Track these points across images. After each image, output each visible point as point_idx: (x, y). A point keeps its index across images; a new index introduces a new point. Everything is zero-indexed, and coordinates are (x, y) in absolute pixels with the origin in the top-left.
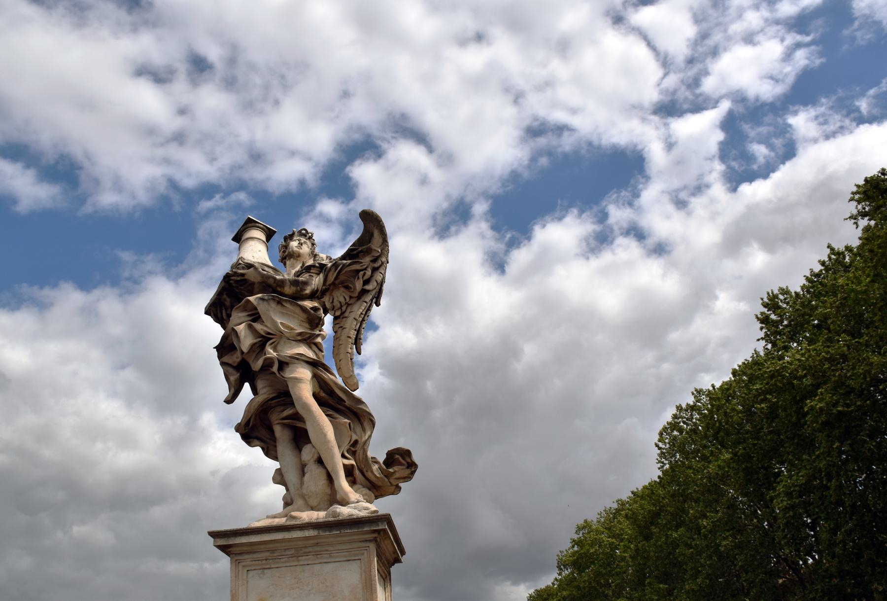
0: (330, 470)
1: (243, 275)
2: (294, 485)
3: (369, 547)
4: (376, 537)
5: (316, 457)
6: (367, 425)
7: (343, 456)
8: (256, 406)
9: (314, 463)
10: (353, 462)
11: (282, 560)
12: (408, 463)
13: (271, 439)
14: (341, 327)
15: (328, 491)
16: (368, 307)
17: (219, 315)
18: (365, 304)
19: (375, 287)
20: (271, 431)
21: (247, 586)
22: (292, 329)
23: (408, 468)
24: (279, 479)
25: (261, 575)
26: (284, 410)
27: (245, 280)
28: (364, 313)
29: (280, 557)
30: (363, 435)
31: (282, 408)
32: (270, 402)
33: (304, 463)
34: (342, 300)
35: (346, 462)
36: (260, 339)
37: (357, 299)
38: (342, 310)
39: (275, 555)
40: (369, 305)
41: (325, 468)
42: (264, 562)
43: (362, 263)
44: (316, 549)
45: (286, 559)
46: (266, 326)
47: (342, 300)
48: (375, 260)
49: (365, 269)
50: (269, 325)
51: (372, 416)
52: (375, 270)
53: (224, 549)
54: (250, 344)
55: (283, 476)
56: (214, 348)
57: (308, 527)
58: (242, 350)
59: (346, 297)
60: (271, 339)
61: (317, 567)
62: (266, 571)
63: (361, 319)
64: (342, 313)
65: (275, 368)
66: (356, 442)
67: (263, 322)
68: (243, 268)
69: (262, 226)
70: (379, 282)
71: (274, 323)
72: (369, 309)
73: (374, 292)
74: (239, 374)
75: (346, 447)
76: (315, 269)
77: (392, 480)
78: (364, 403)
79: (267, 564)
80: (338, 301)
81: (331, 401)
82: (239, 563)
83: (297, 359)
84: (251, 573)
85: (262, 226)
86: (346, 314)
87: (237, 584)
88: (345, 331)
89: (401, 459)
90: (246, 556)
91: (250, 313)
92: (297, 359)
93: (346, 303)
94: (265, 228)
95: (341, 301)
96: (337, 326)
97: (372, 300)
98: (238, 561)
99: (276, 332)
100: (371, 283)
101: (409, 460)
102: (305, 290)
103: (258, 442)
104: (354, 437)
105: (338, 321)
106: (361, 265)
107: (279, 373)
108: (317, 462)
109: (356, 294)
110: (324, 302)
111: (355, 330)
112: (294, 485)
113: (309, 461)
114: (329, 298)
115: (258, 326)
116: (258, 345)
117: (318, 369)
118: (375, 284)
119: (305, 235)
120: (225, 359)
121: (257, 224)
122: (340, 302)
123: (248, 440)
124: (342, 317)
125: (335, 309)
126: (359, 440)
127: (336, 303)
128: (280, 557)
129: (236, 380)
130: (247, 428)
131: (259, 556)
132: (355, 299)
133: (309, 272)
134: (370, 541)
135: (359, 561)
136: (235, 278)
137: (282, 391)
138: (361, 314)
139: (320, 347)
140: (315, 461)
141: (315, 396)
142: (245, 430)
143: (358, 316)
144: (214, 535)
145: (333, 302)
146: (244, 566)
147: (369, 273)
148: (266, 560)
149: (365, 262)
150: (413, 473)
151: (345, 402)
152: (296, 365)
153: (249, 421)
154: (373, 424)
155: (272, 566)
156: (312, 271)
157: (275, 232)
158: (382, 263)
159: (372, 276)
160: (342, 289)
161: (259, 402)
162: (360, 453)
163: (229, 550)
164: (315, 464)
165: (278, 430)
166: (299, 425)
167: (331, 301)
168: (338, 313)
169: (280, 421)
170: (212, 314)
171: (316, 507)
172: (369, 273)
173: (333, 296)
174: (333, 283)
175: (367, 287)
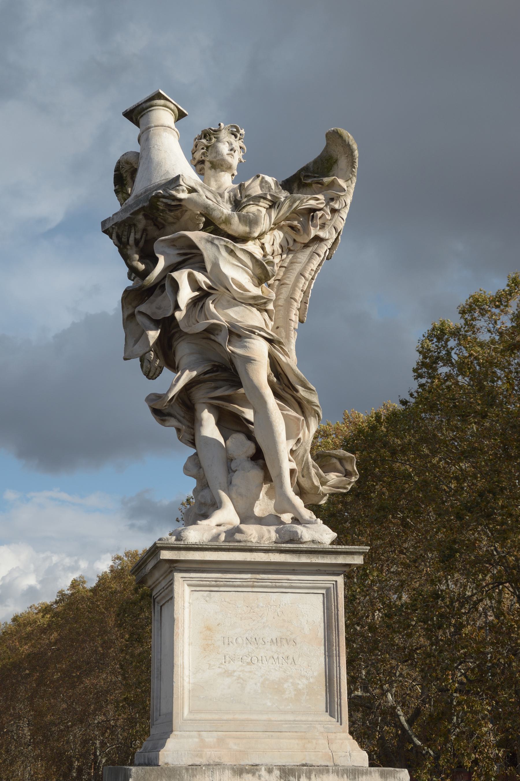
2: (220, 483)
17: (124, 239)
22: (247, 290)
25: (208, 599)
26: (216, 388)
27: (180, 205)
31: (213, 385)
33: (231, 456)
36: (197, 293)
37: (303, 245)
63: (311, 277)
69: (172, 106)
76: (265, 201)
85: (172, 106)
91: (181, 252)
94: (175, 108)
102: (254, 232)
108: (249, 459)
110: (263, 244)
133: (257, 205)
136: (169, 202)
137: (217, 364)
141: (270, 382)
156: (261, 204)
157: (186, 115)
163: (175, 565)
164: (248, 460)
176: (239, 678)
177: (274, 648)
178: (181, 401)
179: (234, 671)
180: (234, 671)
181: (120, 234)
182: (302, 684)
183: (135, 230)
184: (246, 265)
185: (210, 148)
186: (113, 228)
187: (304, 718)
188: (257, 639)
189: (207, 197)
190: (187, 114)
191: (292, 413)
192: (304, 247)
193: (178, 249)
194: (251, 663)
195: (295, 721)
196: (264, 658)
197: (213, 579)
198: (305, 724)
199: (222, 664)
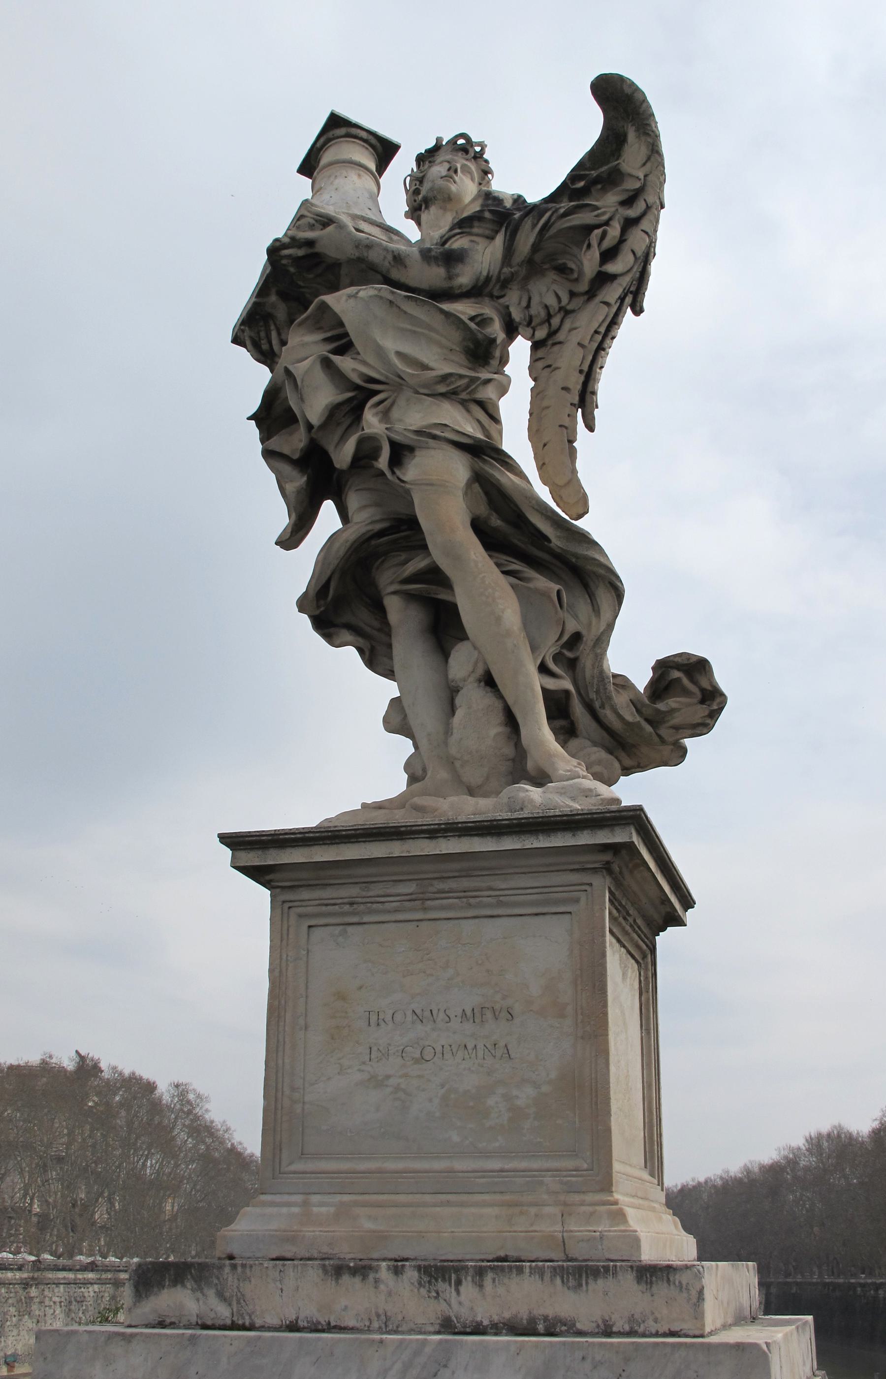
0: (510, 702)
1: (310, 243)
2: (429, 735)
3: (591, 885)
4: (608, 863)
5: (480, 671)
6: (604, 597)
7: (543, 669)
8: (342, 553)
9: (476, 685)
10: (567, 684)
11: (387, 906)
12: (703, 690)
13: (379, 630)
15: (509, 751)
16: (612, 315)
17: (265, 347)
18: (606, 308)
19: (629, 267)
20: (379, 609)
21: (307, 962)
22: (425, 367)
23: (702, 702)
24: (396, 720)
25: (341, 939)
27: (317, 255)
28: (602, 330)
29: (382, 899)
30: (594, 621)
31: (403, 556)
32: (373, 542)
34: (551, 301)
35: (552, 684)
36: (350, 394)
37: (586, 297)
38: (550, 325)
39: (371, 893)
40: (614, 309)
41: (501, 697)
42: (347, 908)
43: (596, 208)
44: (465, 883)
45: (398, 904)
46: (365, 363)
47: (551, 301)
48: (629, 201)
49: (607, 223)
50: (371, 360)
51: (618, 577)
52: (630, 223)
53: (255, 873)
54: (327, 406)
55: (406, 716)
56: (249, 419)
57: (446, 830)
58: (305, 416)
59: (560, 293)
60: (377, 392)
61: (468, 926)
62: (350, 929)
64: (552, 334)
65: (383, 462)
66: (577, 637)
67: (358, 353)
68: (312, 227)
70: (639, 253)
71: (380, 352)
72: (614, 322)
73: (625, 281)
74: (305, 478)
75: (549, 648)
77: (664, 732)
78: (596, 544)
79: (354, 914)
80: (541, 302)
81: (517, 540)
82: (290, 908)
83: (434, 437)
84: (317, 933)
86: (560, 336)
87: (284, 957)
88: (559, 375)
89: (686, 681)
90: (305, 894)
91: (329, 334)
92: (434, 437)
93: (561, 309)
94: (370, 137)
95: (548, 304)
96: (540, 364)
97: (622, 299)
98: (287, 905)
99: (387, 377)
100: (620, 258)
101: (705, 684)
102: (458, 275)
103: (347, 635)
104: (572, 626)
105: (540, 353)
106: (596, 213)
107: (393, 473)
108: (482, 684)
109: (583, 287)
110: (507, 307)
111: (581, 372)
112: (429, 735)
113: (464, 680)
115: (345, 363)
116: (346, 408)
117: (485, 461)
118: (631, 258)
119: (464, 149)
120: (276, 443)
121: (354, 131)
122: (546, 307)
123: (326, 631)
124: (550, 342)
125: (533, 324)
126: (584, 632)
127: (536, 310)
128: (382, 899)
129: (298, 492)
130: (322, 602)
131: (335, 895)
132: (582, 299)
134: (595, 870)
135: (567, 917)
138: (596, 332)
139: (491, 412)
140: (480, 681)
141: (478, 527)
142: (318, 607)
143: (589, 337)
144: (232, 841)
145: (528, 306)
146: (300, 916)
148: (351, 904)
149: (605, 207)
150: (714, 715)
151: (549, 541)
152: (432, 452)
153: (326, 587)
154: (618, 594)
155: (365, 919)
156: (475, 230)
158: (648, 207)
159: (622, 241)
160: (552, 275)
161: (347, 541)
162: (587, 662)
165: (394, 606)
166: (443, 596)
167: (524, 303)
168: (541, 334)
170: (248, 342)
171: (479, 787)
172: (614, 231)
173: (528, 291)
174: (530, 261)
175: (611, 268)
176: (397, 1089)
177: (469, 1027)
179: (388, 1077)
180: (388, 1077)
181: (257, 339)
182: (525, 1096)
183: (275, 324)
184: (430, 328)
186: (243, 331)
187: (524, 1165)
188: (435, 1013)
189: (358, 230)
191: (542, 582)
193: (325, 332)
194: (422, 1059)
195: (502, 1171)
196: (447, 1049)
197: (346, 901)
198: (523, 1177)
199: (364, 1063)
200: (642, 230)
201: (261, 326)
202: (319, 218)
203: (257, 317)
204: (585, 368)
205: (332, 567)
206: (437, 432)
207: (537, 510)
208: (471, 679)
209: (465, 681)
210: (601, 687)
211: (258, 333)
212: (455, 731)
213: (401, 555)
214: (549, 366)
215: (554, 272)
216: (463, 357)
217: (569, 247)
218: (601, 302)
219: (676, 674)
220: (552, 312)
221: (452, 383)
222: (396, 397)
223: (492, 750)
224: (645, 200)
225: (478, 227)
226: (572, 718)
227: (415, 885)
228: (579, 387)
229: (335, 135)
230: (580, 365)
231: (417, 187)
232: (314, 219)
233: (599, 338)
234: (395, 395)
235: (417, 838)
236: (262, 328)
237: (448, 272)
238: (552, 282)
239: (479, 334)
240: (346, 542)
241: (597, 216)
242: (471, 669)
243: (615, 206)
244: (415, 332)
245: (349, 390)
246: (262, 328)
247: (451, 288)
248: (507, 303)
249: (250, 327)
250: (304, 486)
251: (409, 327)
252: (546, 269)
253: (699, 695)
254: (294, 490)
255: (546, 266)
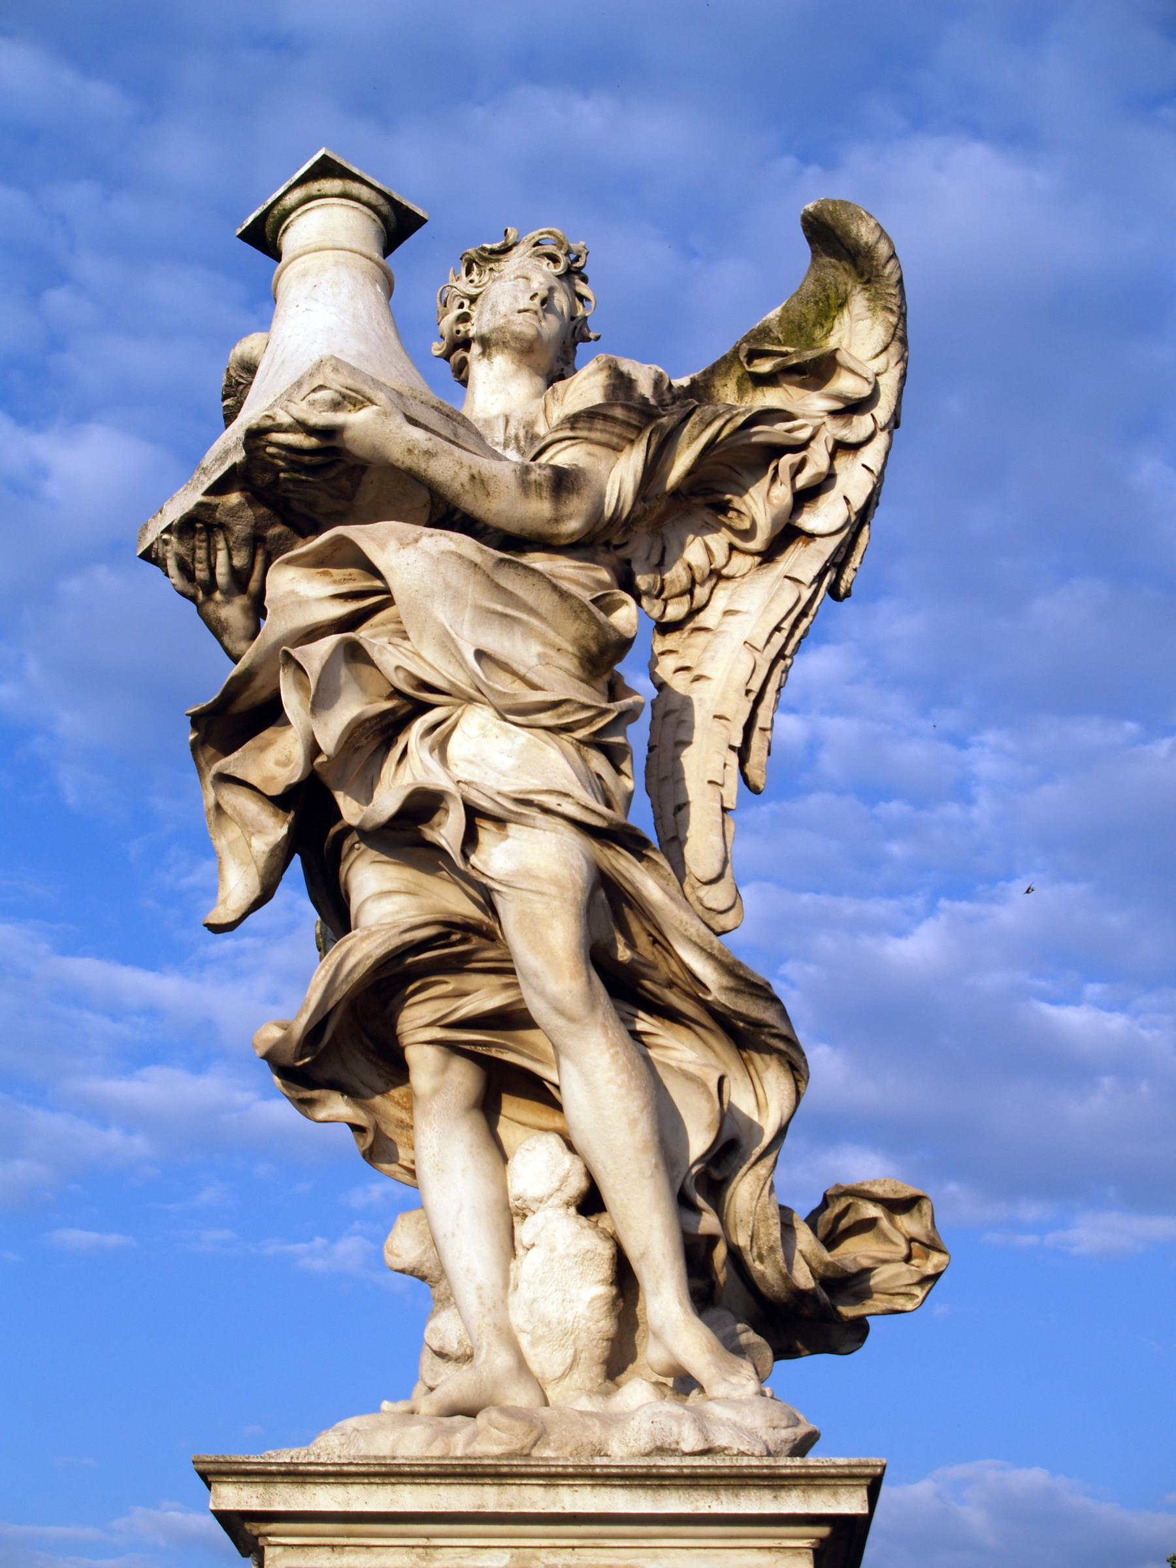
1: (328, 433)
2: (479, 1288)
14: (686, 669)
15: (606, 1325)
17: (201, 574)
28: (786, 625)
49: (804, 446)
54: (349, 724)
64: (693, 613)
71: (448, 644)
76: (609, 426)
83: (546, 811)
86: (705, 619)
89: (884, 1223)
92: (546, 811)
95: (693, 564)
97: (820, 577)
108: (573, 1210)
109: (757, 544)
110: (628, 562)
112: (479, 1288)
114: (651, 548)
124: (691, 625)
125: (663, 596)
138: (778, 629)
140: (568, 1204)
147: (818, 459)
149: (804, 416)
157: (421, 221)
161: (368, 957)
167: (655, 559)
168: (676, 610)
169: (437, 1033)
170: (171, 564)
173: (662, 536)
174: (676, 492)
175: (809, 521)
178: (371, 1046)
181: (189, 560)
183: (226, 540)
185: (479, 301)
190: (426, 217)
192: (760, 564)
193: (335, 582)
200: (864, 466)
201: (202, 541)
202: (349, 392)
203: (199, 525)
204: (756, 686)
205: (338, 996)
206: (551, 801)
207: (696, 944)
208: (555, 1201)
209: (541, 1202)
210: (762, 1230)
211: (193, 550)
212: (523, 1286)
213: (446, 982)
214: (686, 669)
215: (708, 510)
216: (575, 661)
217: (737, 473)
218: (786, 577)
219: (871, 1211)
220: (698, 577)
221: (567, 713)
222: (459, 717)
223: (584, 1321)
224: (872, 415)
225: (602, 431)
226: (714, 1278)
227: (508, 1557)
228: (743, 719)
229: (323, 192)
230: (747, 683)
231: (465, 309)
232: (340, 393)
233: (779, 639)
234: (459, 712)
235: (525, 1484)
236: (204, 544)
237: (556, 510)
238: (702, 526)
239: (612, 632)
240: (368, 958)
241: (789, 431)
242: (556, 1185)
243: (821, 417)
244: (506, 616)
245: (389, 697)
246: (204, 544)
247: (558, 535)
248: (629, 557)
249: (180, 539)
250: (282, 845)
251: (499, 608)
252: (695, 504)
253: (903, 1250)
254: (267, 849)
255: (699, 501)
